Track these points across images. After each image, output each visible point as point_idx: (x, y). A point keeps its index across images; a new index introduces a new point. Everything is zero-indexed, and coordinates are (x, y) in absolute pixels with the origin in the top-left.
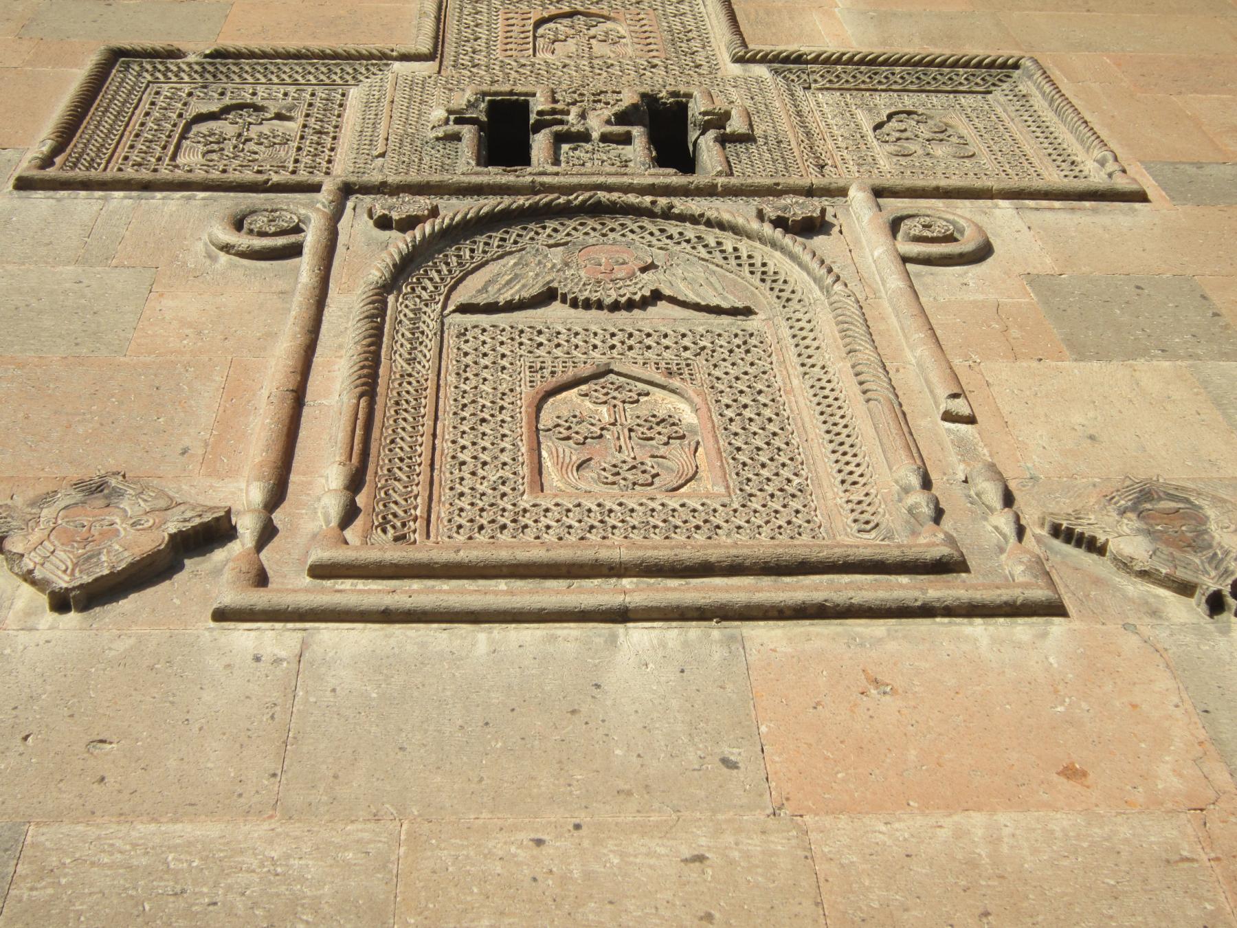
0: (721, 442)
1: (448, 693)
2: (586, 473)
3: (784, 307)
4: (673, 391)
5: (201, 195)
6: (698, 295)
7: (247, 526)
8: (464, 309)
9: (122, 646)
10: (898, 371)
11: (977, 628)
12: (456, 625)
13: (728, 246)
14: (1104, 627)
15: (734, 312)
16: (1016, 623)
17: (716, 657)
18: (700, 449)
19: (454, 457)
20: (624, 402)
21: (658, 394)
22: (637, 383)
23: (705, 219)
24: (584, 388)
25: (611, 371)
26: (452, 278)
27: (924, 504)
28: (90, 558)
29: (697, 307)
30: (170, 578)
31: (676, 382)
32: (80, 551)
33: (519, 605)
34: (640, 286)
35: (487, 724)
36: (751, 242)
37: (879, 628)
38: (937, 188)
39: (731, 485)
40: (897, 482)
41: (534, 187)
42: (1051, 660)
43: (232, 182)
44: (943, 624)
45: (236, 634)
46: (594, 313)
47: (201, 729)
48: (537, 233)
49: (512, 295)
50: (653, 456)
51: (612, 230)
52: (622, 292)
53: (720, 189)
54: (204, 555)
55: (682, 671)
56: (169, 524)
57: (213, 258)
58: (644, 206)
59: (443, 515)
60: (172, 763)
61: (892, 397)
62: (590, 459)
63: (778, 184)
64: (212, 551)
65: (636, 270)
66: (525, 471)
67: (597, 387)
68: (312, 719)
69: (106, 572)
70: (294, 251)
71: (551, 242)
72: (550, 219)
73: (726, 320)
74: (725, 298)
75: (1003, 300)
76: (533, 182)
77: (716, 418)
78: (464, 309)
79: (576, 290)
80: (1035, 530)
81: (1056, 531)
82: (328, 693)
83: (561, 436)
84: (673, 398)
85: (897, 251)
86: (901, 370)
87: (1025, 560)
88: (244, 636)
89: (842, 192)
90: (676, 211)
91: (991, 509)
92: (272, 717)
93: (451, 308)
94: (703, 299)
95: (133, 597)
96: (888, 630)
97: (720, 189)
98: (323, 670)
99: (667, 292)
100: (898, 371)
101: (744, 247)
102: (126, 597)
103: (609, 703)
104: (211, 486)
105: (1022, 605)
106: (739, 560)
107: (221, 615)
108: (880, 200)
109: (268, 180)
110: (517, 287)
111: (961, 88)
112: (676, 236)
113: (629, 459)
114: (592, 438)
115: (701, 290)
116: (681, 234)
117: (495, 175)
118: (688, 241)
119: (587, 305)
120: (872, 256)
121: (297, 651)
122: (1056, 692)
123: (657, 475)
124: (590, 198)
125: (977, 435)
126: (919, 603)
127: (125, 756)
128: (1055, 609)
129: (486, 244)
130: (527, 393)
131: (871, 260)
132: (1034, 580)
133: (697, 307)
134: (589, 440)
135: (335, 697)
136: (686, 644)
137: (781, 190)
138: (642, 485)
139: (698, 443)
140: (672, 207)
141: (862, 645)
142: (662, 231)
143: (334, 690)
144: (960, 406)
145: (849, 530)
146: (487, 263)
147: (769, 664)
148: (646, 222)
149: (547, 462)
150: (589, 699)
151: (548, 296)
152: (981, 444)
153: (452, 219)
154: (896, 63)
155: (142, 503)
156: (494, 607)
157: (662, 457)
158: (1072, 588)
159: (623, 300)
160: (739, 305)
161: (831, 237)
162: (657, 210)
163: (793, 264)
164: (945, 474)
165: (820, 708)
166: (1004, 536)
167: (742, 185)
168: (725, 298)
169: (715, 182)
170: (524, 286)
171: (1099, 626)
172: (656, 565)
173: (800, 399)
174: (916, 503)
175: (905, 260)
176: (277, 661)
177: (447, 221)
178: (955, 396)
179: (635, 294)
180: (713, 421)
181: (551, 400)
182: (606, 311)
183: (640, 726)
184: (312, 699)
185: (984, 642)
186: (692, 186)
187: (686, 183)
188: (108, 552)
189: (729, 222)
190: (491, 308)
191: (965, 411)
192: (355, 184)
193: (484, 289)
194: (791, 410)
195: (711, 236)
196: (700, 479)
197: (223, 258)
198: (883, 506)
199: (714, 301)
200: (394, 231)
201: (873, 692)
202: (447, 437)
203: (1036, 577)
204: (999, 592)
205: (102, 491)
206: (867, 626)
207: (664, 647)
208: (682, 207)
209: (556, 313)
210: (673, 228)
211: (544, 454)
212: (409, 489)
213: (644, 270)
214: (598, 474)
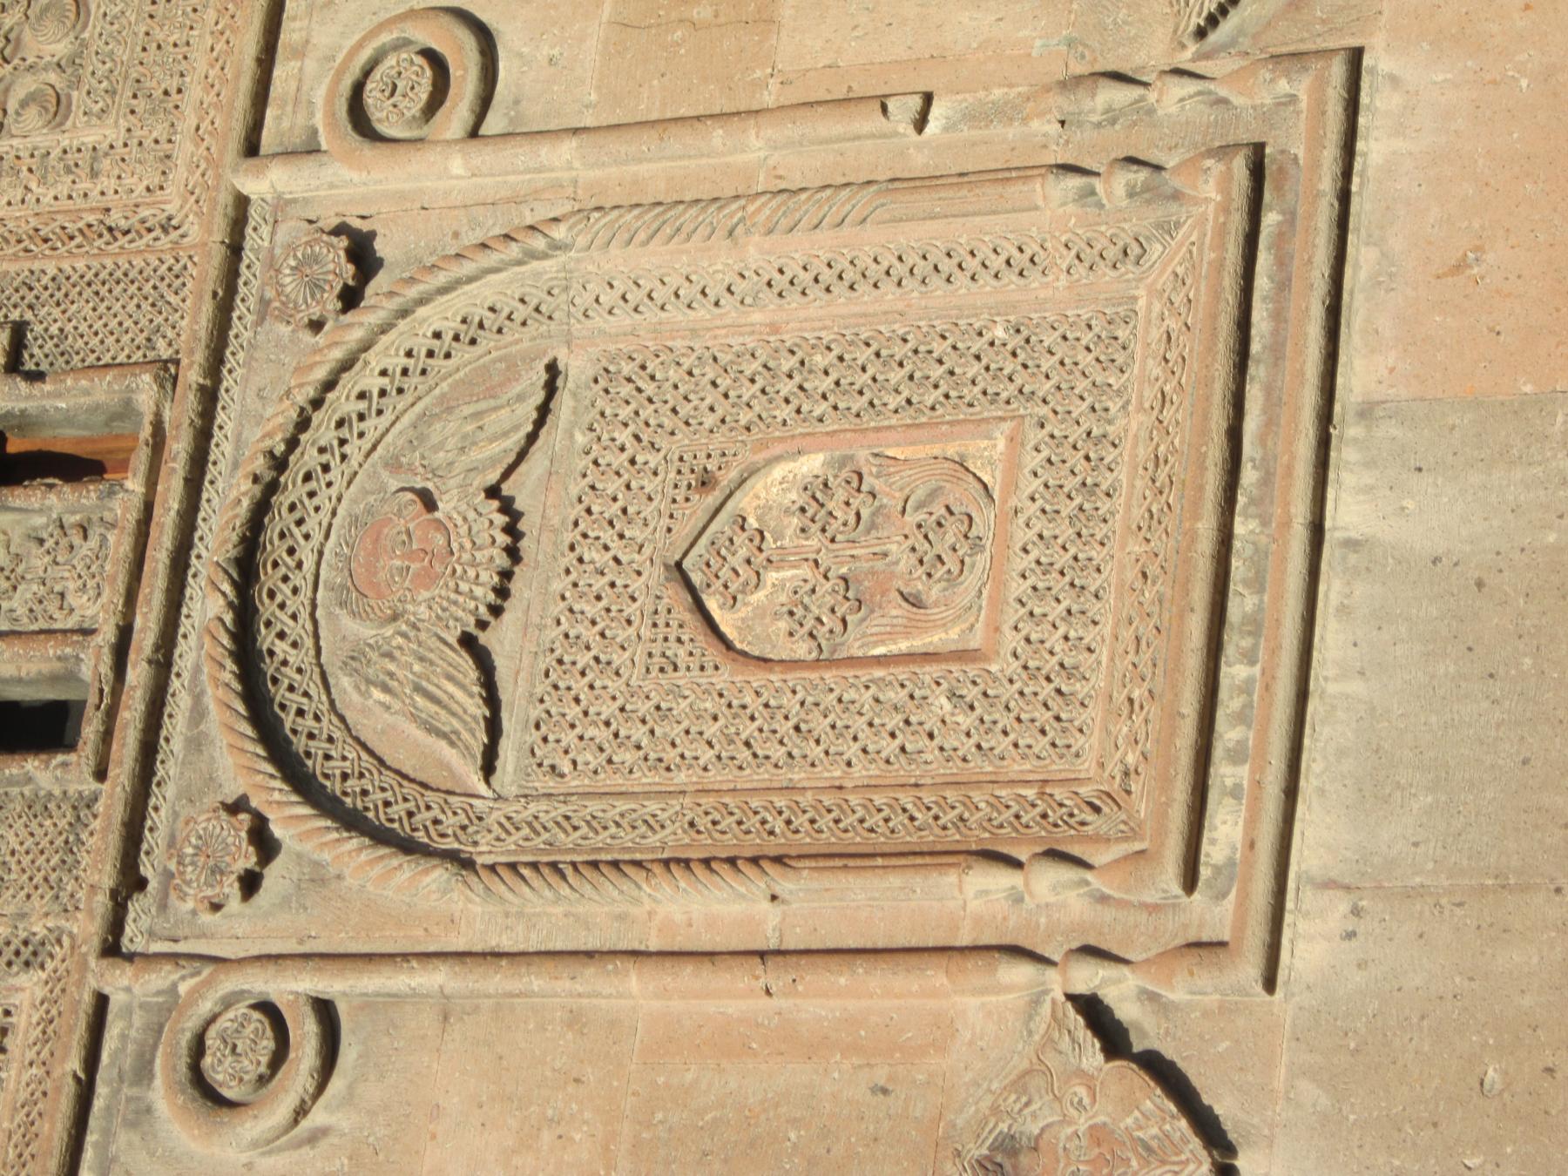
0: (893, 422)
1: (1434, 719)
2: (934, 592)
3: (550, 318)
4: (743, 481)
6: (506, 434)
7: (1088, 977)
8: (488, 769)
9: (1308, 1091)
10: (780, 177)
11: (1371, 148)
12: (1308, 718)
13: (374, 383)
14: (1386, 13)
15: (551, 388)
16: (1368, 108)
17: (1395, 432)
18: (890, 453)
19: (888, 762)
20: (760, 549)
21: (744, 502)
22: (713, 527)
23: (309, 409)
24: (712, 604)
25: (679, 565)
26: (401, 785)
27: (1131, 176)
28: (1148, 1148)
29: (532, 438)
30: (1172, 1064)
31: (728, 477)
32: (1134, 1163)
33: (1295, 642)
34: (471, 515)
35: (1491, 676)
36: (377, 348)
37: (1361, 255)
38: (259, 61)
39: (1000, 413)
40: (1064, 204)
41: (158, 662)
42: (1440, 78)
43: (70, 1135)
44: (1361, 185)
45: (1298, 963)
46: (515, 586)
47: (1471, 979)
48: (285, 663)
49: (471, 695)
50: (904, 511)
51: (291, 551)
52: (483, 538)
53: (208, 382)
54: (1126, 1031)
55: (1420, 470)
56: (1085, 1064)
57: (314, 1138)
58: (258, 495)
59: (1028, 767)
60: (1527, 1001)
61: (874, 188)
62: (901, 594)
63: (215, 294)
64: (1119, 1023)
65: (429, 516)
66: (930, 671)
67: (718, 584)
68: (1465, 862)
69: (1183, 1123)
70: (325, 1011)
71: (309, 642)
72: (255, 640)
73: (564, 405)
74: (520, 398)
76: (150, 662)
77: (820, 428)
78: (488, 769)
79: (472, 605)
80: (1184, 59)
81: (1201, 33)
82: (1420, 850)
83: (839, 628)
84: (757, 485)
85: (456, 141)
86: (781, 172)
87: (1268, 76)
88: (1298, 956)
89: (242, 202)
90: (280, 449)
91: (1142, 99)
92: (1460, 905)
93: (482, 788)
94: (516, 428)
95: (1206, 1100)
96: (1367, 244)
97: (208, 382)
98: (1376, 860)
99: (493, 477)
100: (780, 177)
101: (375, 359)
102: (1210, 1108)
103: (1468, 548)
104: (971, 1043)
105: (1349, 92)
106: (1229, 396)
107: (1270, 984)
108: (263, 151)
109: (75, 1077)
110: (451, 688)
112: (325, 458)
113: (909, 542)
114: (847, 589)
115: (490, 430)
116: (322, 450)
117: (90, 730)
118: (342, 442)
119: (502, 592)
120: (458, 177)
121: (1340, 893)
122: (1494, 82)
123: (948, 508)
124: (226, 572)
125: (959, 97)
126: (1336, 204)
127: (1512, 1053)
128: (1356, 57)
129: (311, 736)
130: (726, 676)
131: (463, 183)
132: (1312, 73)
133: (532, 438)
134: (850, 594)
135: (1428, 840)
136: (1369, 464)
137: (225, 291)
138: (970, 526)
139: (876, 455)
140: (271, 453)
141: (1391, 275)
142: (308, 477)
143: (1416, 844)
144: (904, 109)
145: (1131, 276)
146: (357, 740)
147: (1417, 376)
148: (282, 500)
149: (903, 646)
150: (1458, 569)
152: (981, 94)
153: (272, 776)
155: (1034, 1107)
156: (1295, 670)
157: (906, 501)
158: (1306, 35)
159: (503, 539)
160: (544, 376)
161: (380, 231)
162: (268, 476)
163: (459, 291)
164: (1045, 146)
165: (1498, 328)
166: (1199, 93)
167: (208, 347)
168: (520, 398)
169: (194, 386)
170: (450, 678)
171: (1383, 19)
172: (1225, 491)
173: (802, 314)
174: (1127, 184)
175: (474, 133)
176: (1356, 912)
177: (278, 784)
178: (884, 109)
179: (491, 522)
180: (835, 432)
181: (738, 646)
182: (516, 569)
183: (1510, 516)
184: (1430, 865)
185: (1400, 144)
186: (198, 422)
187: (191, 430)
188: (1140, 1128)
189: (331, 373)
190: (494, 727)
191: (916, 102)
192: (105, 940)
193: (450, 738)
194: (824, 328)
195: (342, 402)
196: (962, 456)
197: (318, 1117)
198: (1103, 228)
199: (527, 412)
200: (266, 872)
201: (1475, 270)
202: (838, 773)
203: (1307, 70)
204: (1330, 113)
205: (1000, 1166)
206: (1357, 266)
207: (1372, 488)
208: (279, 437)
209: (501, 640)
210: (307, 458)
211: (880, 650)
212: (982, 805)
214: (939, 581)
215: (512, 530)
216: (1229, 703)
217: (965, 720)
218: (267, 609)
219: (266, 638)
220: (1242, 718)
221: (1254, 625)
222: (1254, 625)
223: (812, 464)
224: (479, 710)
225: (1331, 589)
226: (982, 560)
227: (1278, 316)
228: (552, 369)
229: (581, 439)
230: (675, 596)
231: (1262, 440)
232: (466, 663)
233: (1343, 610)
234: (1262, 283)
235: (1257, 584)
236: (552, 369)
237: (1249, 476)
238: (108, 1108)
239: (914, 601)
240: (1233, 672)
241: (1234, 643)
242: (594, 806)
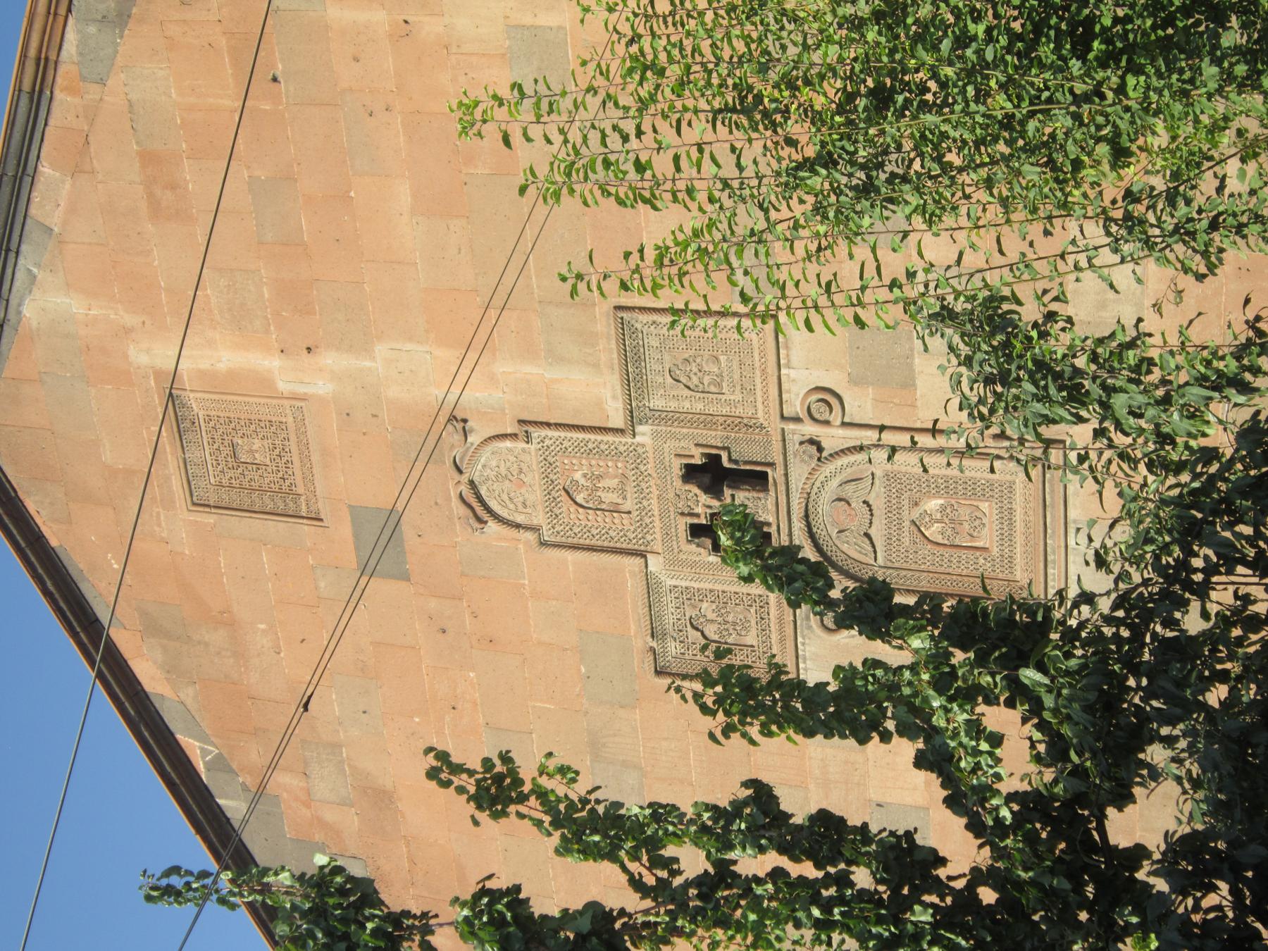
5: (800, 639)
24: (923, 529)
75: (871, 396)
111: (641, 343)
119: (871, 523)
149: (969, 544)
151: (867, 535)
154: (627, 371)
190: (875, 552)
213: (849, 504)
215: (871, 510)
216: (1050, 578)
217: (989, 565)
218: (813, 523)
219: (815, 530)
220: (1054, 580)
221: (1054, 562)
222: (1054, 562)
223: (941, 501)
224: (870, 549)
225: (1071, 558)
226: (986, 529)
227: (1052, 498)
228: (873, 474)
229: (883, 490)
230: (913, 528)
231: (1051, 524)
232: (866, 540)
233: (1074, 562)
234: (1047, 490)
235: (1054, 553)
236: (873, 474)
237: (1049, 531)
238: (801, 625)
239: (971, 536)
240: (1050, 571)
241: (1050, 566)
242: (904, 573)
